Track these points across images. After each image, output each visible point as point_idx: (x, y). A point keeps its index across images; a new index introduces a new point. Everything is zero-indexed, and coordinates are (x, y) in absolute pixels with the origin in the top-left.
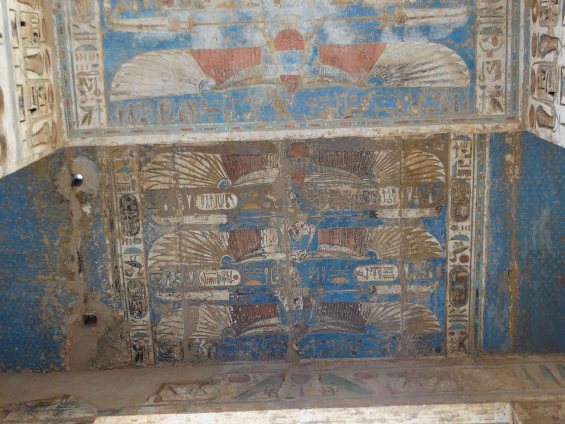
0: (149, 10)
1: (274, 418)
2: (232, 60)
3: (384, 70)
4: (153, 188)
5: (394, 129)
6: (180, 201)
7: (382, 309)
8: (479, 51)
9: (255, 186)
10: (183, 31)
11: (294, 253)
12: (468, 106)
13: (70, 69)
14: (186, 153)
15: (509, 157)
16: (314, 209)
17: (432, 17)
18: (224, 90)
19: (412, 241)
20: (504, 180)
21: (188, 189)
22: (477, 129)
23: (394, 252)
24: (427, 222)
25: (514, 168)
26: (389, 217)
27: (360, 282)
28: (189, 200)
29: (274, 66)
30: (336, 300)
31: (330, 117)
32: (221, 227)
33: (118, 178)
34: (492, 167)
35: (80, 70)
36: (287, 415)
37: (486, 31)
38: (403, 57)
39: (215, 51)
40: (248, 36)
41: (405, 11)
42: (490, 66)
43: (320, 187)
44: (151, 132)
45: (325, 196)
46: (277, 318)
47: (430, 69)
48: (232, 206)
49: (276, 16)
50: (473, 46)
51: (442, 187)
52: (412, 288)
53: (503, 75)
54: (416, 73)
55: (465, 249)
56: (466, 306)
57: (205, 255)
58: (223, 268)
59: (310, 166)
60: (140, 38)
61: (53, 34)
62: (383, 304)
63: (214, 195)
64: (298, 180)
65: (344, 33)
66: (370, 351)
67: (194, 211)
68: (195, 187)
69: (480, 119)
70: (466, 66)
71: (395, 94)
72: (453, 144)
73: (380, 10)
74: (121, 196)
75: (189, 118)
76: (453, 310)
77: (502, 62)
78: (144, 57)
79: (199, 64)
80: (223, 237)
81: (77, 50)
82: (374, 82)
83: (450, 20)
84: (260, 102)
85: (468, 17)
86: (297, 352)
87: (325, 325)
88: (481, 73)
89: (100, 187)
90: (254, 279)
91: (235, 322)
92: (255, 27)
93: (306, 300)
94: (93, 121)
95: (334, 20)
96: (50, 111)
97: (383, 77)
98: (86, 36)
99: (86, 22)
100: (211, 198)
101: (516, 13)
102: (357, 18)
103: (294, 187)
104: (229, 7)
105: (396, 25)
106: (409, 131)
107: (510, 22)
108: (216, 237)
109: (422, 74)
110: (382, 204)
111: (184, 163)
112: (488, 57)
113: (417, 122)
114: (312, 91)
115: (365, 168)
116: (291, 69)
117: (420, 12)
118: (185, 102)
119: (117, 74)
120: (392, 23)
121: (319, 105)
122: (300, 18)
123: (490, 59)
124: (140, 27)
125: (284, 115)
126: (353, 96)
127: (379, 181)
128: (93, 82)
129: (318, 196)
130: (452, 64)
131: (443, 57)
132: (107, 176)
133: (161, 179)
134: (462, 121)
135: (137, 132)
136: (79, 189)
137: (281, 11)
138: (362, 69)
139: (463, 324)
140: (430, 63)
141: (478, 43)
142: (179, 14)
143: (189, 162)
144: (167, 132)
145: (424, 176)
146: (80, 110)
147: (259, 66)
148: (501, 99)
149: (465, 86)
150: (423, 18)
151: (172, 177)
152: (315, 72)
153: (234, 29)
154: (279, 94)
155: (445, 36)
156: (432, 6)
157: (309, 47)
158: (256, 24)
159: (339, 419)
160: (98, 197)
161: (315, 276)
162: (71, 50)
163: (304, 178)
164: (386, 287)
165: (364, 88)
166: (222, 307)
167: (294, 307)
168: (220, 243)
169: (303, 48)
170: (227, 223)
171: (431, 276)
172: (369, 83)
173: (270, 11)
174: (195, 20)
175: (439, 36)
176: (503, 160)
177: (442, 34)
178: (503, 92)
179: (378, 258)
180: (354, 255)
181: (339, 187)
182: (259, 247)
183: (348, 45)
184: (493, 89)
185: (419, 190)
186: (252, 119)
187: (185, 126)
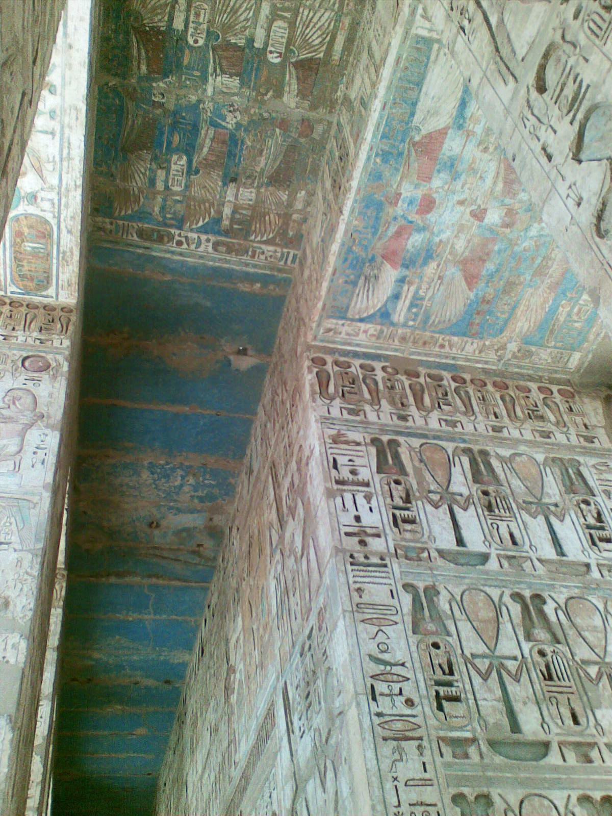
1: (76, 109)
6: (287, 4)
7: (143, 171)
8: (369, 326)
10: (466, 125)
11: (211, 104)
14: (332, 24)
15: (258, 285)
16: (250, 131)
18: (407, 146)
19: (202, 207)
21: (297, 16)
23: (195, 191)
24: (218, 220)
26: (228, 193)
27: (171, 157)
28: (286, 14)
30: (157, 132)
31: (355, 223)
32: (251, 40)
36: (79, 121)
37: (382, 332)
39: (441, 147)
40: (442, 175)
42: (357, 331)
46: (146, 71)
47: (368, 296)
48: (270, 56)
52: (159, 199)
55: (188, 245)
56: (135, 238)
57: (225, 16)
58: (208, 32)
59: (289, 136)
62: (148, 173)
63: (284, 41)
65: (416, 244)
66: (100, 152)
67: (274, 16)
72: (279, 250)
75: (394, 111)
76: (133, 227)
78: (460, 85)
80: (240, 39)
84: (386, 173)
86: (107, 84)
87: (133, 116)
90: (191, 59)
91: (147, 29)
93: (161, 105)
94: (422, 20)
100: (282, 37)
102: (423, 254)
103: (273, 118)
108: (242, 32)
110: (241, 189)
111: (323, 19)
113: (332, 281)
115: (276, 181)
116: (404, 201)
117: (410, 295)
118: (409, 111)
122: (440, 217)
123: (362, 331)
127: (263, 190)
130: (367, 308)
135: (398, 62)
137: (450, 204)
139: (120, 234)
140: (373, 294)
142: (482, 124)
143: (323, 25)
144: (388, 88)
145: (258, 226)
148: (331, 333)
150: (406, 297)
152: (395, 218)
153: (452, 166)
154: (388, 189)
157: (413, 217)
159: (70, 169)
161: (184, 118)
163: (280, 129)
164: (163, 178)
166: (166, 18)
167: (155, 92)
168: (235, 34)
169: (417, 213)
170: (253, 47)
171: (169, 216)
174: (471, 137)
175: (388, 303)
176: (257, 282)
177: (389, 305)
179: (192, 177)
180: (198, 157)
181: (264, 158)
182: (223, 72)
184: (340, 330)
187: (388, 107)
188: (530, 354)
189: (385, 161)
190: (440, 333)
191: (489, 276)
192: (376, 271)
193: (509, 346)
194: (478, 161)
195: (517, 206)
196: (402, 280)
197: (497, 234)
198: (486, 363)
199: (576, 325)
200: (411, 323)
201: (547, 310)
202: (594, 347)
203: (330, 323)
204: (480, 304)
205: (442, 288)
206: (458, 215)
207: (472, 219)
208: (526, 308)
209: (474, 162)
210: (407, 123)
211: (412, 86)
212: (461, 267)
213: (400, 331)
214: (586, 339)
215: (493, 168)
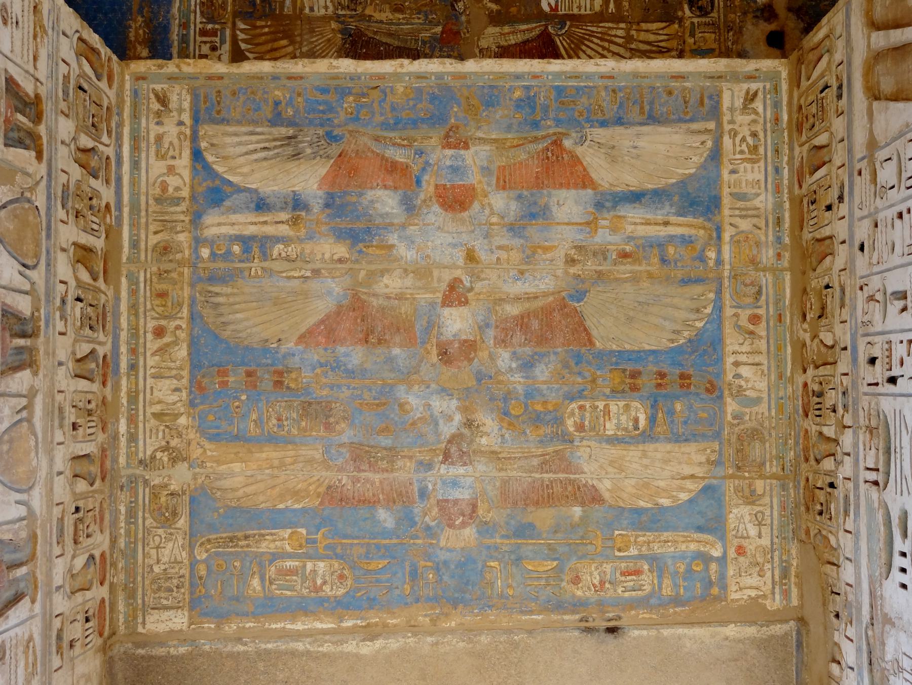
0: (652, 246)
2: (537, 172)
3: (321, 152)
4: (664, 24)
5: (308, 69)
8: (186, 174)
9: (515, 22)
10: (606, 215)
12: (202, 99)
13: (770, 168)
17: (252, 223)
18: (551, 131)
20: (151, 20)
21: (612, 22)
22: (189, 64)
25: (136, 37)
28: (612, 5)
29: (477, 164)
31: (400, 88)
33: (715, 39)
34: (168, 39)
35: (756, 166)
37: (177, 201)
38: (293, 170)
39: (561, 186)
40: (514, 206)
41: (291, 233)
42: (171, 153)
43: (419, 18)
44: (658, 76)
45: (413, 5)
49: (473, 232)
50: (195, 182)
51: (240, 12)
53: (152, 140)
54: (275, 147)
60: (667, 208)
61: (791, 217)
63: (576, 11)
64: (451, 30)
65: (377, 205)
68: (601, 25)
69: (184, 78)
70: (205, 153)
71: (307, 118)
73: (325, 236)
74: (712, 15)
75: (603, 94)
77: (154, 158)
79: (585, 170)
81: (758, 195)
82: (336, 136)
83: (228, 218)
84: (500, 112)
85: (202, 221)
88: (183, 143)
89: (741, 28)
92: (503, 218)
95: (392, 224)
96: (802, 101)
97: (323, 142)
98: (744, 213)
99: (742, 232)
100: (579, 7)
101: (134, 225)
102: (360, 225)
103: (457, 18)
104: (539, 247)
105: (303, 214)
106: (286, 66)
107: (143, 213)
109: (267, 145)
112: (173, 166)
113: (275, 77)
114: (425, 126)
117: (270, 230)
118: (607, 117)
119: (703, 159)
120: (309, 217)
121: (415, 105)
123: (172, 162)
124: (666, 224)
125: (466, 93)
126: (367, 118)
127: (334, 25)
128: (738, 149)
129: (422, 5)
130: (225, 158)
131: (236, 168)
132: (730, 43)
133: (652, 38)
134: (210, 78)
136: (773, 27)
137: (465, 237)
138: (353, 155)
141: (188, 186)
142: (610, 238)
144: (636, 75)
145: (266, 30)
146: (760, 110)
147: (499, 164)
148: (156, 106)
149: (206, 127)
150: (265, 223)
151: (635, 40)
152: (420, 153)
153: (533, 216)
154: (472, 123)
155: (235, 196)
156: (253, 238)
158: (502, 222)
160: (745, 13)
162: (766, 195)
163: (442, 32)
165: (351, 129)
169: (437, 186)
172: (344, 135)
173: (481, 239)
174: (588, 229)
177: (239, 199)
178: (152, 116)
181: (391, 17)
183: (371, 188)
185: (275, 9)
186: (512, 90)
187: (609, 83)
188: (168, 518)
189: (519, 104)
190: (192, 317)
191: (337, 361)
192: (309, 151)
193: (182, 467)
194: (549, 256)
195: (484, 354)
196: (297, 204)
197: (423, 343)
198: (132, 438)
199: (256, 582)
200: (205, 253)
201: (281, 506)
202: (207, 647)
203: (180, 98)
204: (273, 369)
205: (296, 283)
206: (447, 260)
207: (444, 286)
208: (276, 463)
209: (546, 249)
210: (588, 120)
211: (647, 108)
212: (345, 302)
213: (182, 237)
214: (222, 617)
215: (542, 287)
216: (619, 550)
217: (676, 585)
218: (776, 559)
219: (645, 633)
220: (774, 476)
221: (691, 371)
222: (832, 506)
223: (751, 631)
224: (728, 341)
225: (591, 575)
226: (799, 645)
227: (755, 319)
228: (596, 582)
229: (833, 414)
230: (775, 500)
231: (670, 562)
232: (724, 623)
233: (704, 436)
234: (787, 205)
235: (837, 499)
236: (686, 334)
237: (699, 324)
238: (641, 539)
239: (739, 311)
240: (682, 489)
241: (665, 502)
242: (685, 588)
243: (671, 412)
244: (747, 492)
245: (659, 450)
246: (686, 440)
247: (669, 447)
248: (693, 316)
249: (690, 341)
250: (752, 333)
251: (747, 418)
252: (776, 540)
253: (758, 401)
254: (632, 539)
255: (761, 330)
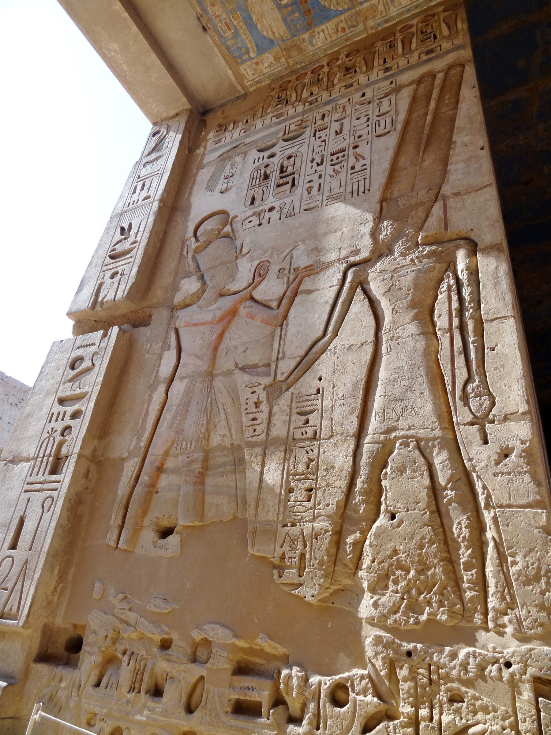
81: (395, 7)
96: (436, 18)
98: (386, 5)
216: (233, 17)
217: (233, 46)
218: (261, 77)
219: (211, 42)
220: (288, 64)
221: (312, 13)
222: (280, 106)
223: (233, 79)
224: (330, 23)
225: (218, 10)
226: (238, 98)
227: (343, 30)
228: (217, 14)
229: (310, 94)
230: (280, 68)
231: (239, 39)
232: (231, 69)
233: (290, 31)
234: (394, 22)
235: (282, 108)
236: (326, 4)
237: (332, 8)
238: (241, 24)
239: (344, 22)
240: (267, 31)
241: (259, 27)
242: (234, 49)
243: (293, 12)
244: (278, 56)
245: (277, 14)
246: (285, 24)
247: (280, 18)
248: (335, 3)
249: (324, 7)
250: (337, 31)
251: (305, 44)
252: (267, 74)
253: (313, 45)
254: (239, 20)
255: (340, 34)
